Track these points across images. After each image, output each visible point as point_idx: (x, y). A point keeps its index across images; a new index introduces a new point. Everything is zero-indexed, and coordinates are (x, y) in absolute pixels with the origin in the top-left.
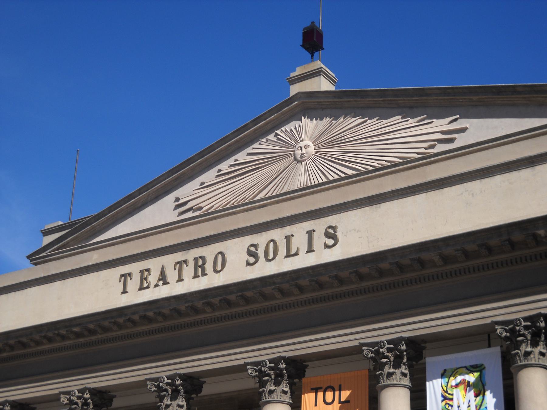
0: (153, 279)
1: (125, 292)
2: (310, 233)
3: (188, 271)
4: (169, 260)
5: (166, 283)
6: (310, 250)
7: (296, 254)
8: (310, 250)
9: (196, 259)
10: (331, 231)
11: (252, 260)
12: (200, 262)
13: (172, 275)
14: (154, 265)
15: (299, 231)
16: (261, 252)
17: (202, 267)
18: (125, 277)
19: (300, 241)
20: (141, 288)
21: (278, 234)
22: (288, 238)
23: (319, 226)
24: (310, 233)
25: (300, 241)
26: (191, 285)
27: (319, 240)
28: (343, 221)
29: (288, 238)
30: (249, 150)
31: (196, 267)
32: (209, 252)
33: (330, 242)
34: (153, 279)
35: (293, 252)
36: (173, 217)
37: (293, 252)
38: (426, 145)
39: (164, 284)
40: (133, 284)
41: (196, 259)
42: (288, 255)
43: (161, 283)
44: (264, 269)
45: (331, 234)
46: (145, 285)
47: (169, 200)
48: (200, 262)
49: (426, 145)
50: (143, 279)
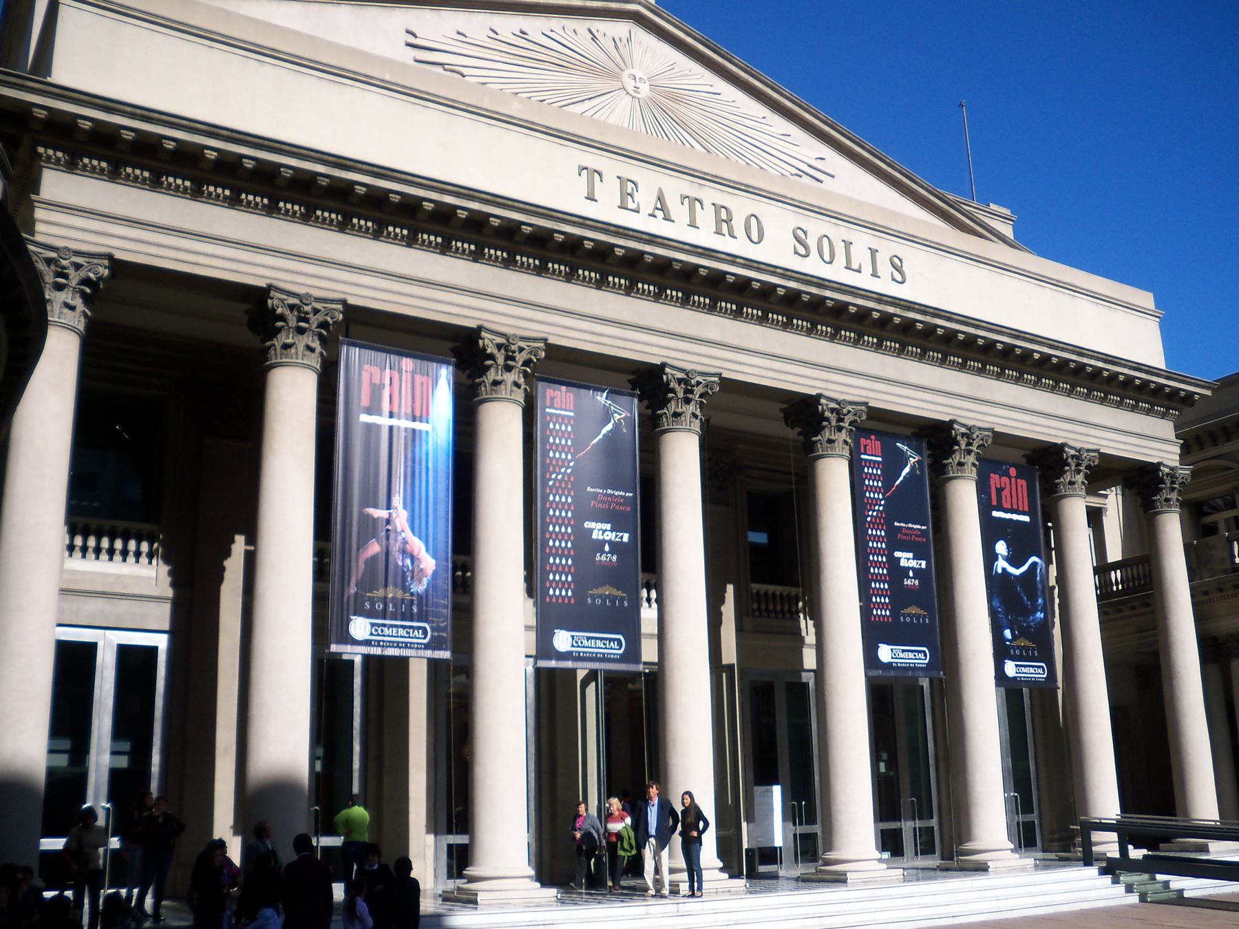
0: (645, 198)
1: (591, 198)
2: (873, 252)
3: (706, 217)
5: (667, 218)
6: (875, 275)
7: (859, 271)
8: (875, 274)
9: (718, 208)
10: (896, 260)
11: (802, 250)
12: (724, 215)
13: (680, 212)
14: (649, 182)
15: (862, 241)
16: (812, 242)
17: (728, 221)
19: (860, 256)
20: (623, 207)
21: (839, 232)
22: (847, 245)
23: (888, 248)
24: (873, 252)
25: (860, 256)
26: (705, 237)
27: (885, 269)
28: (914, 258)
29: (847, 245)
31: (719, 221)
32: (741, 206)
33: (898, 277)
34: (645, 198)
35: (855, 266)
37: (855, 266)
38: (795, 171)
39: (665, 219)
40: (608, 192)
41: (718, 208)
42: (848, 268)
43: (660, 214)
46: (631, 205)
48: (724, 215)
49: (795, 171)
50: (625, 195)
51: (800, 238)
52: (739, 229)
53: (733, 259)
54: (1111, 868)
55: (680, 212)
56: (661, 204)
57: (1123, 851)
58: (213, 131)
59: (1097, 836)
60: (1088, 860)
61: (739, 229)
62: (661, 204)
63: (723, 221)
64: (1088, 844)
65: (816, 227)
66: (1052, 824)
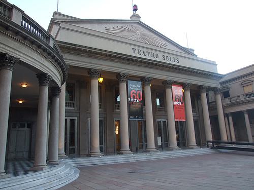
0: (142, 52)
3: (150, 55)
4: (146, 50)
13: (146, 54)
14: (142, 50)
15: (173, 57)
18: (134, 49)
21: (169, 55)
23: (176, 57)
25: (172, 59)
26: (150, 58)
27: (176, 61)
30: (125, 25)
34: (142, 52)
36: (105, 31)
40: (136, 52)
44: (165, 61)
45: (177, 60)
47: (104, 26)
51: (163, 56)
52: (155, 56)
53: (155, 61)
54: (212, 148)
55: (146, 54)
56: (144, 53)
57: (213, 145)
58: (83, 46)
59: (209, 143)
60: (208, 147)
61: (155, 56)
62: (144, 53)
63: (153, 55)
64: (208, 145)
65: (166, 55)
66: (201, 142)
